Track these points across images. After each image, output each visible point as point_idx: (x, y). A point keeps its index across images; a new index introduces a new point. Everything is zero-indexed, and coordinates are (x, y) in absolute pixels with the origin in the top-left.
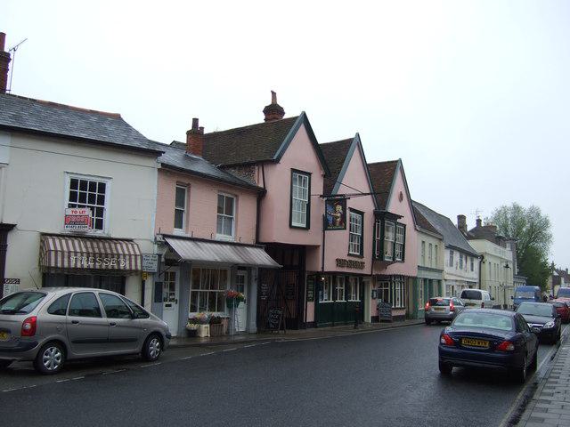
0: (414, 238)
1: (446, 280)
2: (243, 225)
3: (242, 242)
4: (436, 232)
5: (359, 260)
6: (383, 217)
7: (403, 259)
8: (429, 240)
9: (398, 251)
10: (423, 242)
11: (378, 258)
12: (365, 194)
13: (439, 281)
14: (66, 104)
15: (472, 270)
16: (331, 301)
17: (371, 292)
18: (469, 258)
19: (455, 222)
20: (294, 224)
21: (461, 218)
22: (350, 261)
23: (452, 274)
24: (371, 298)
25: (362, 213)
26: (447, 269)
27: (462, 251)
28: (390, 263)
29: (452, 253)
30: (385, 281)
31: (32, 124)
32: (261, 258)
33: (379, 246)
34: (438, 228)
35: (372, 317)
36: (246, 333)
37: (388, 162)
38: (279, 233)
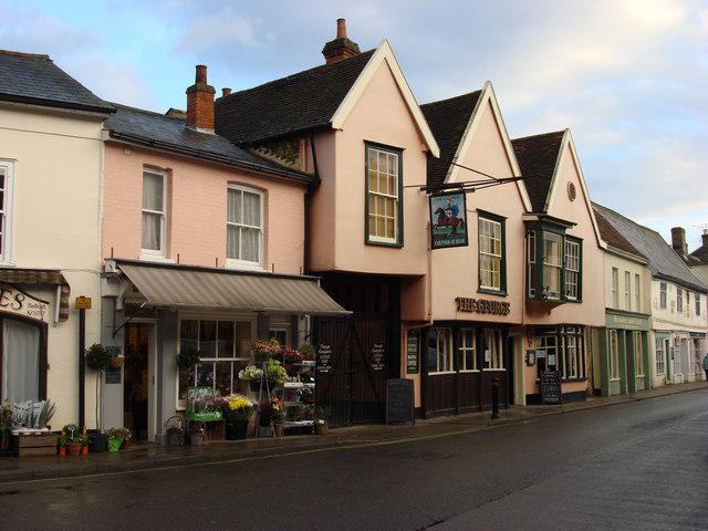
0: (598, 266)
1: (655, 331)
2: (282, 247)
3: (277, 271)
4: (635, 252)
5: (500, 300)
6: (541, 226)
7: (579, 300)
8: (623, 266)
9: (569, 283)
10: (615, 269)
11: (537, 301)
12: (501, 181)
13: (644, 333)
14: (74, 76)
15: (698, 313)
16: (452, 372)
17: (524, 354)
18: (692, 295)
19: (669, 240)
20: (372, 238)
21: (678, 233)
22: (483, 302)
23: (665, 322)
24: (524, 364)
25: (502, 219)
26: (656, 313)
27: (680, 284)
28: (555, 304)
29: (663, 287)
30: (551, 336)
31: (498, 239)
32: (320, 301)
33: (534, 274)
34: (639, 246)
35: (528, 396)
36: (699, 381)
37: (551, 134)
38: (350, 253)
